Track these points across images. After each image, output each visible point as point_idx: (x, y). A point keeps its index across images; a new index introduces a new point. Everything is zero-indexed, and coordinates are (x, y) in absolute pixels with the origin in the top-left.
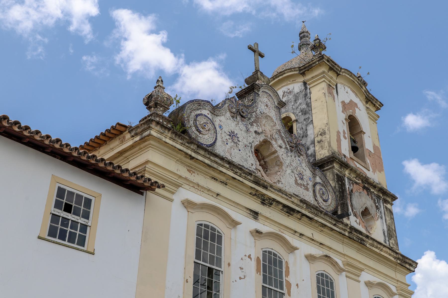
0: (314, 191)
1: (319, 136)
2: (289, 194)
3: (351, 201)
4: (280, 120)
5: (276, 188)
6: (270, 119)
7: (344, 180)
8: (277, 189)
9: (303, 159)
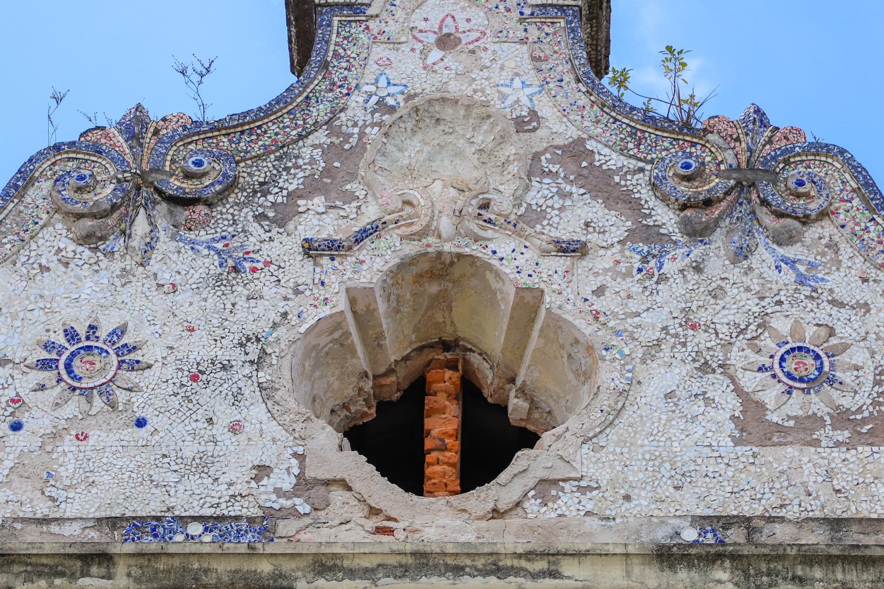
2: (519, 556)
4: (578, 81)
5: (374, 561)
6: (462, 112)
8: (392, 560)
9: (836, 238)
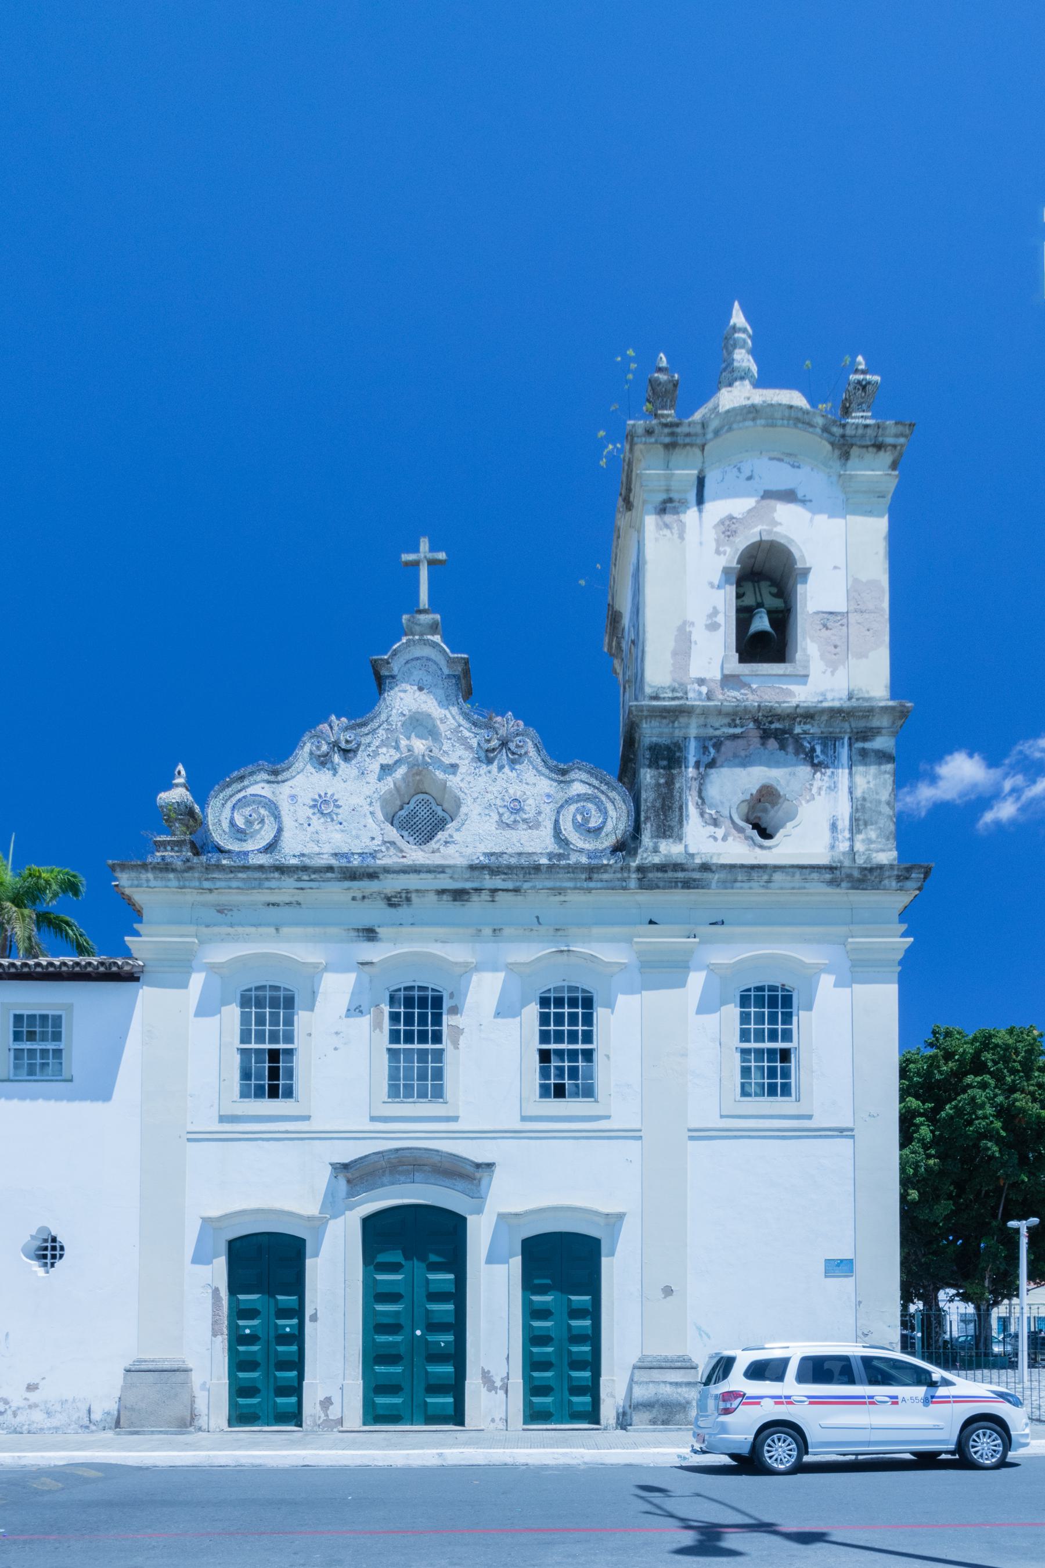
3: (700, 792)
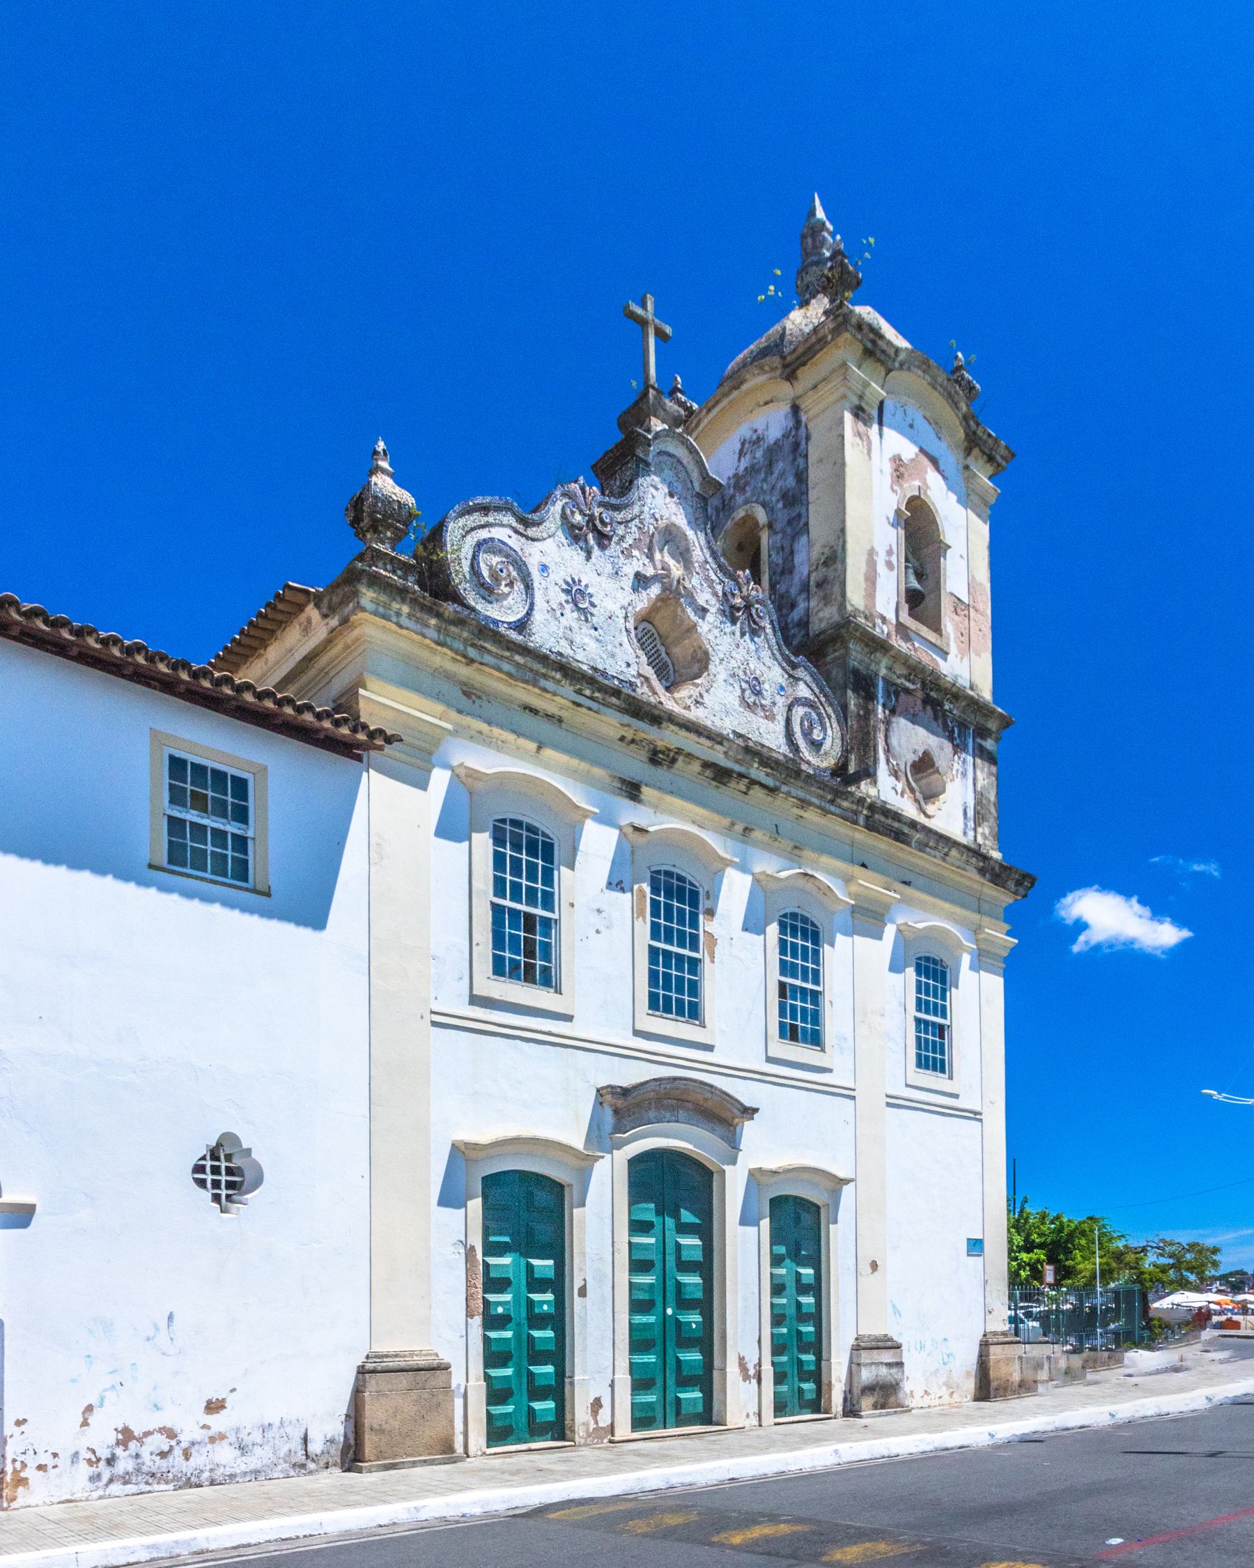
0: (788, 722)
1: (820, 567)
3: (886, 737)
7: (875, 686)
